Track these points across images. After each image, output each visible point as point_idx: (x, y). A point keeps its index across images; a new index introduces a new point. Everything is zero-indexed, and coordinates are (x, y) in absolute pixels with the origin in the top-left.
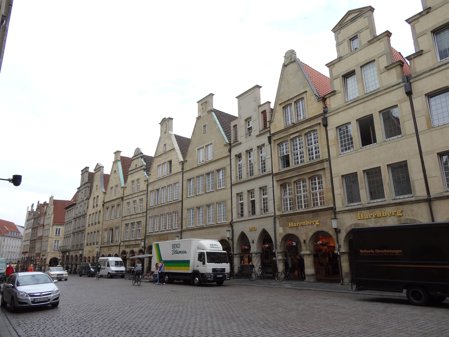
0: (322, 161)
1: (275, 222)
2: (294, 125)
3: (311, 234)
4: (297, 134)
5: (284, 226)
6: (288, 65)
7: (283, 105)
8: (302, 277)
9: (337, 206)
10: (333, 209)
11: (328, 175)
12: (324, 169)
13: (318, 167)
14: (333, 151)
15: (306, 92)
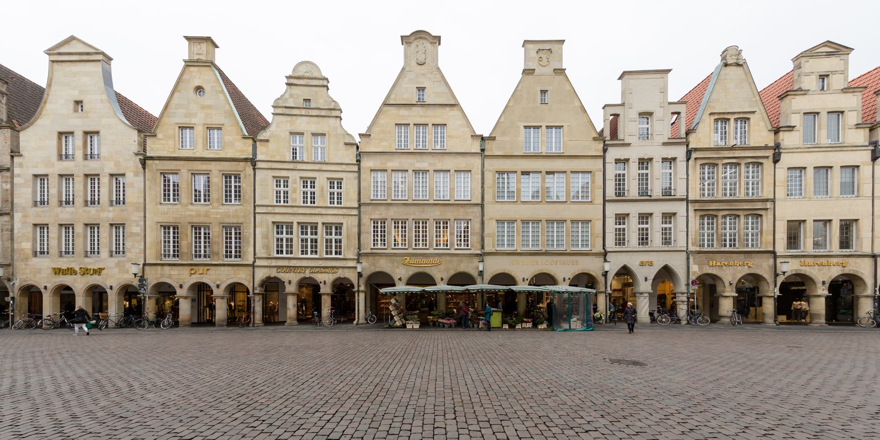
0: (767, 200)
1: (688, 259)
2: (733, 148)
3: (739, 276)
4: (734, 161)
5: (700, 265)
6: (731, 65)
7: (716, 117)
8: (715, 317)
9: (777, 250)
10: (773, 253)
11: (771, 217)
12: (767, 209)
13: (759, 205)
14: (781, 193)
15: (754, 112)
